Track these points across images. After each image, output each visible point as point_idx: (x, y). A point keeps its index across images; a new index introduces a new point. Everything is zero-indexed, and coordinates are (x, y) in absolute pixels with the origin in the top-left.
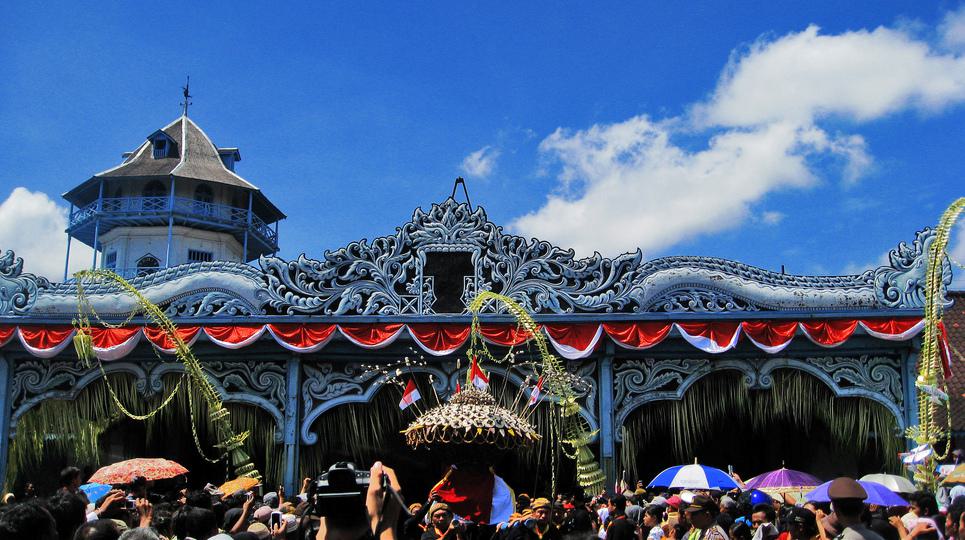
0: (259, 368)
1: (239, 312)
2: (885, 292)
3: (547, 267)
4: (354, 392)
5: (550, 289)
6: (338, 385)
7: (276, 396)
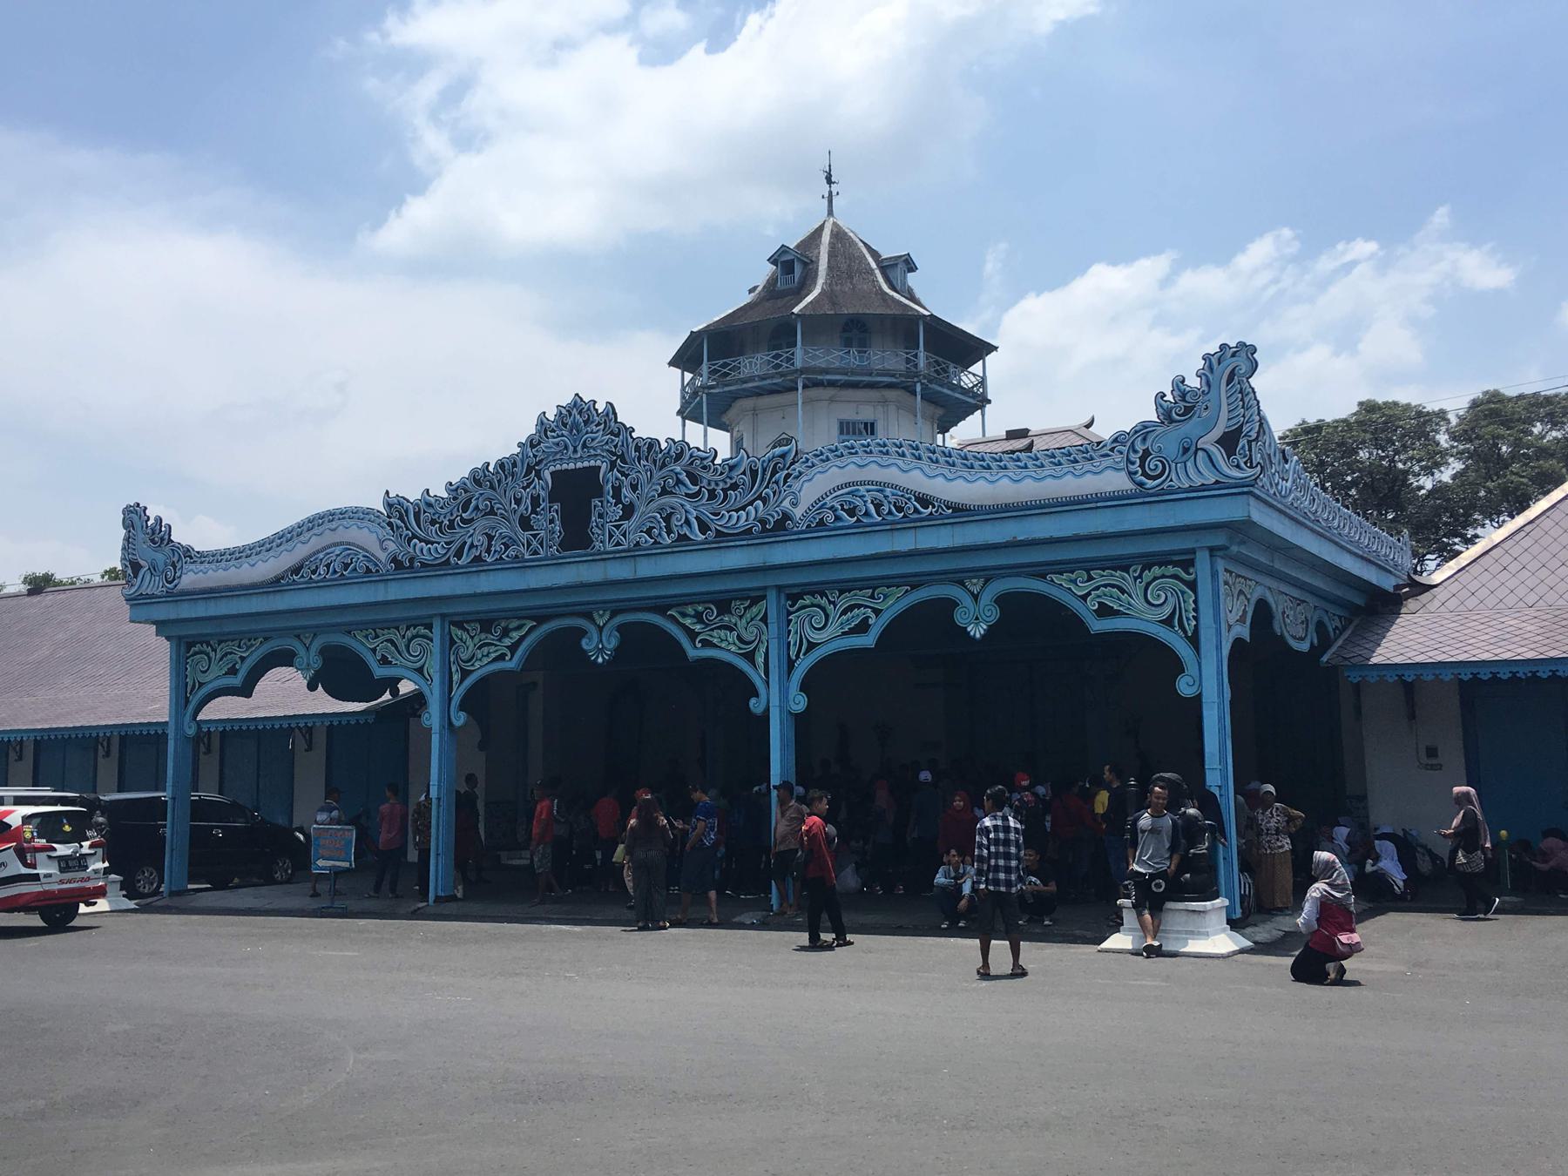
1: (368, 570)
2: (1142, 466)
3: (683, 477)
4: (501, 657)
5: (688, 507)
6: (485, 650)
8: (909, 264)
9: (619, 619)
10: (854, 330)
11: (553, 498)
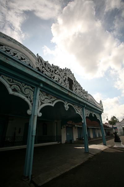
0: (26, 86)
1: (29, 65)
4: (50, 103)
6: (47, 100)
7: (30, 98)
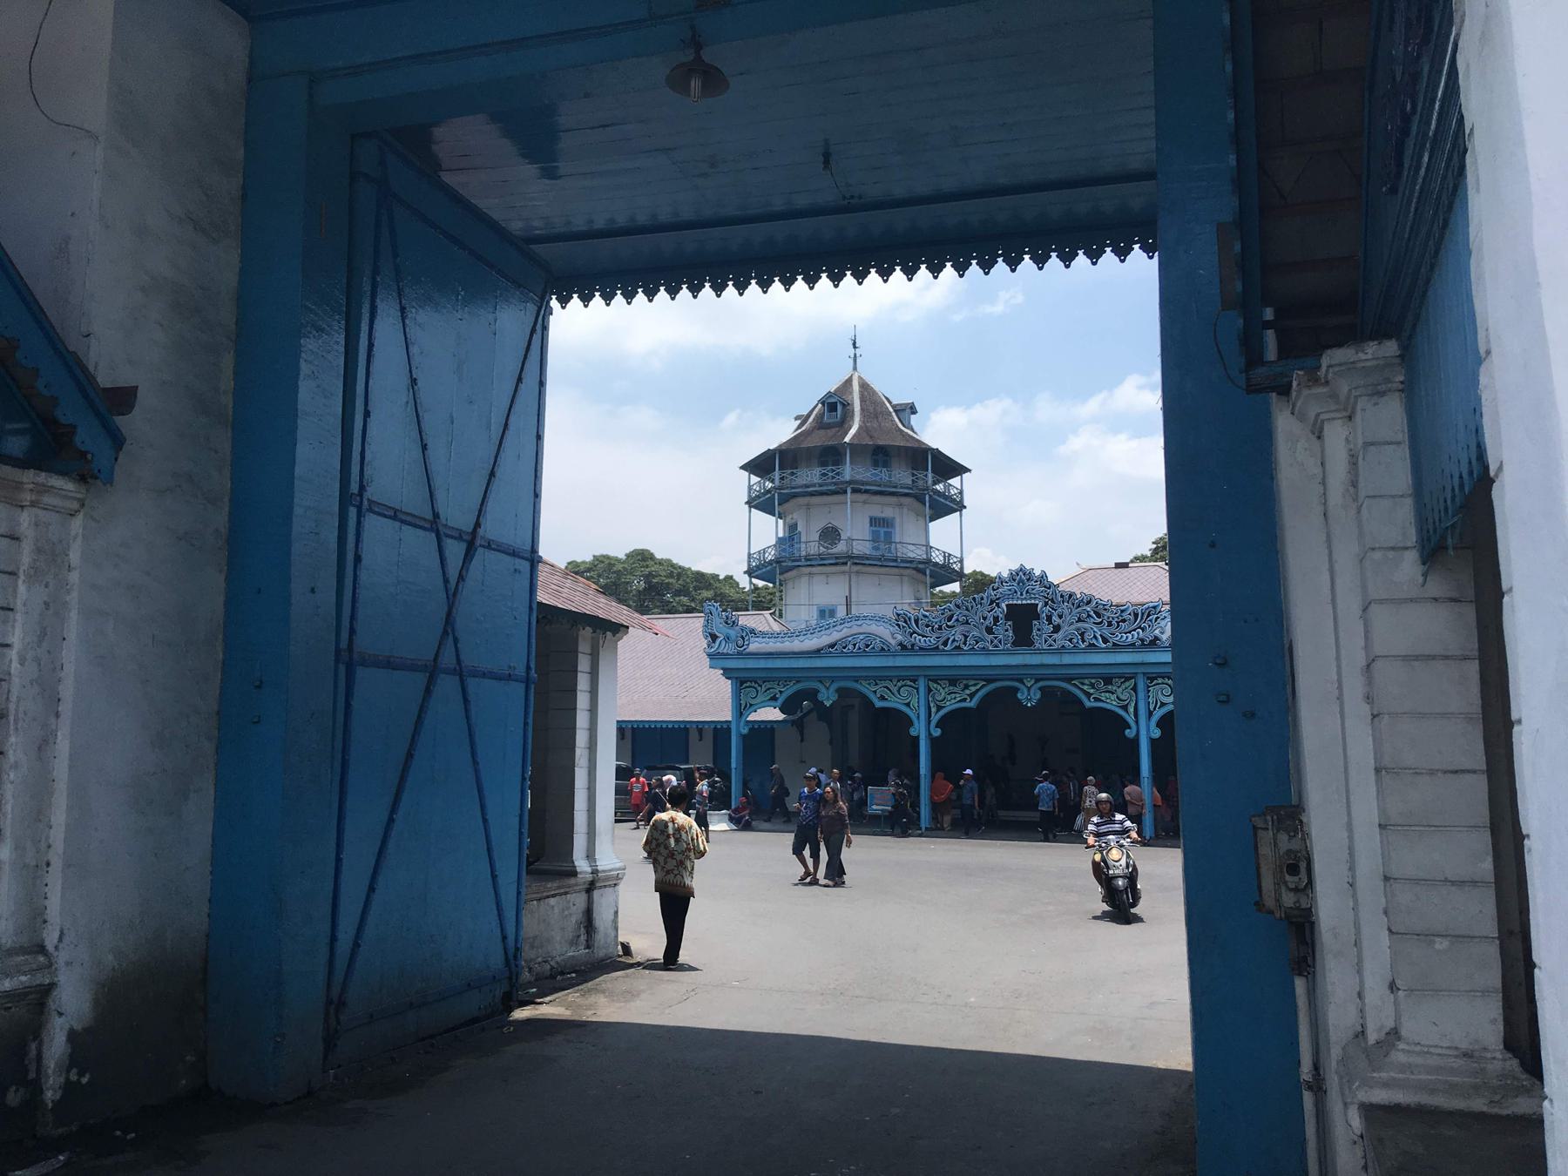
8: (913, 410)
9: (1041, 684)
10: (881, 455)
11: (1007, 618)
